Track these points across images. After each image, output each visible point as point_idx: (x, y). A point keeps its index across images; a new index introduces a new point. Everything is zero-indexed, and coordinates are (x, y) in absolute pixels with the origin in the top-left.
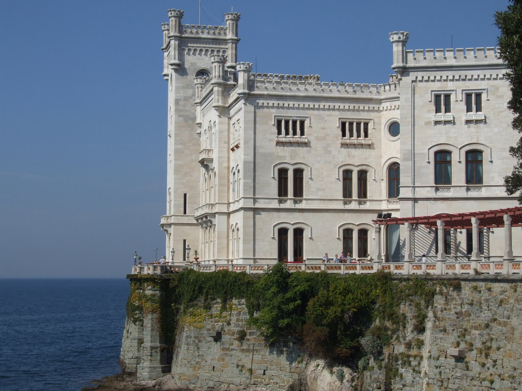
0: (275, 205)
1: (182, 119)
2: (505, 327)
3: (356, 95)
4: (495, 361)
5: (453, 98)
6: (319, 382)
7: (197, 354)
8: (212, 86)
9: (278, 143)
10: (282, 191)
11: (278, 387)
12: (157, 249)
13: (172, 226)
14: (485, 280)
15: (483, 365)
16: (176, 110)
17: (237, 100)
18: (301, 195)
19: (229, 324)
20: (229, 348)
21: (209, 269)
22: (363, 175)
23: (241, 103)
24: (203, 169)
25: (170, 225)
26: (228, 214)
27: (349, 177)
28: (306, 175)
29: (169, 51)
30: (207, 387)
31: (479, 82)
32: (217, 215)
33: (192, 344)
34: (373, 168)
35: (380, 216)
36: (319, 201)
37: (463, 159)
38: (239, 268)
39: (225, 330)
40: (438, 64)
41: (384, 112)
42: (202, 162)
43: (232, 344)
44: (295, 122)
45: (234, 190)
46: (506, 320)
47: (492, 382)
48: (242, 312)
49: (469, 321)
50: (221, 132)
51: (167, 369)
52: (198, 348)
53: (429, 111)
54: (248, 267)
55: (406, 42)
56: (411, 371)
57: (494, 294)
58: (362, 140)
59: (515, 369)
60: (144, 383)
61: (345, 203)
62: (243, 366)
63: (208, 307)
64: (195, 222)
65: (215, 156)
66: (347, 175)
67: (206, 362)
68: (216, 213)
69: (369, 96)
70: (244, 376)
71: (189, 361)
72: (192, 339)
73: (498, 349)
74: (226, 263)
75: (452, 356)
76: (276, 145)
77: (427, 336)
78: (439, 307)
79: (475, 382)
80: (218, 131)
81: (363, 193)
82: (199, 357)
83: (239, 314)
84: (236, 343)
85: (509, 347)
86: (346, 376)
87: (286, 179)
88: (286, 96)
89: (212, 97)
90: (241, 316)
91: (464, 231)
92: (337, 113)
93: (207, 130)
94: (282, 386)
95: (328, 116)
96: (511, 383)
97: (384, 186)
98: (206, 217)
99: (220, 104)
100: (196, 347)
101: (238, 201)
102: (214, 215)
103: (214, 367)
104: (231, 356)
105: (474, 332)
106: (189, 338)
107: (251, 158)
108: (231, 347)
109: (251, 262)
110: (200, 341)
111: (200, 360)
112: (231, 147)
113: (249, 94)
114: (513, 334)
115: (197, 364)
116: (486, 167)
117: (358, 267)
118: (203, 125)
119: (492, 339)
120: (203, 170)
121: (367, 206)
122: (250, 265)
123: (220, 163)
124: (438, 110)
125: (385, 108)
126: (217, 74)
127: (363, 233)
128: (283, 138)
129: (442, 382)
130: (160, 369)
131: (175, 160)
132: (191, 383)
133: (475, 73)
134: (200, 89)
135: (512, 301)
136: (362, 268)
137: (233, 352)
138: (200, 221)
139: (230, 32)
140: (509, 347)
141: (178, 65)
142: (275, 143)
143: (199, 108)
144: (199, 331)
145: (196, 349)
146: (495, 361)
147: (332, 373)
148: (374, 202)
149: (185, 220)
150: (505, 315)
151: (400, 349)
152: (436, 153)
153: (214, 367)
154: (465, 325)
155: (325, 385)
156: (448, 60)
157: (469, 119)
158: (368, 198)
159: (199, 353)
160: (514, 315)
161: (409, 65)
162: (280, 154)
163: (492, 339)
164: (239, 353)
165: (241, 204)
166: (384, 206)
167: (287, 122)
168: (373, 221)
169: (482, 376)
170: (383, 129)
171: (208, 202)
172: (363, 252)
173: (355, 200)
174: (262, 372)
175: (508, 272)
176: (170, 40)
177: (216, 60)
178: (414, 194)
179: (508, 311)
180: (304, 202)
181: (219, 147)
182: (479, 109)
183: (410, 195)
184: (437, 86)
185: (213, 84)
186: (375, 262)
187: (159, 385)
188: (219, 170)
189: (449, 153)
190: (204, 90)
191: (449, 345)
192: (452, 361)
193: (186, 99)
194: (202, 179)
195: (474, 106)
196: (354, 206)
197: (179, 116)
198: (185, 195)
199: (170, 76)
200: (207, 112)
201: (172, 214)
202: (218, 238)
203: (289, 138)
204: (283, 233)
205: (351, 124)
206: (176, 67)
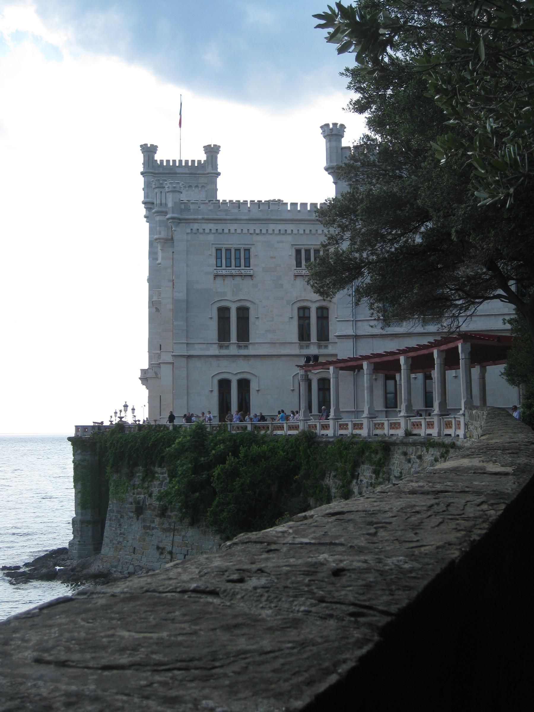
0: (214, 350)
7: (119, 532)
9: (216, 276)
14: (414, 444)
19: (150, 495)
20: (150, 526)
30: (127, 571)
32: (162, 365)
33: (115, 519)
39: (147, 504)
43: (153, 522)
48: (164, 483)
51: (98, 546)
52: (120, 525)
57: (425, 465)
61: (301, 347)
62: (163, 549)
63: (131, 475)
67: (127, 541)
71: (110, 540)
72: (115, 514)
76: (215, 279)
78: (365, 481)
82: (121, 536)
83: (161, 485)
84: (157, 520)
88: (225, 220)
90: (163, 487)
92: (290, 238)
95: (278, 242)
100: (118, 524)
104: (152, 535)
106: (111, 512)
107: (182, 296)
108: (153, 525)
111: (121, 540)
113: (180, 219)
115: (118, 544)
126: (158, 201)
130: (91, 547)
132: (112, 567)
137: (154, 531)
139: (209, 166)
144: (122, 505)
145: (118, 526)
158: (330, 342)
159: (120, 530)
162: (219, 290)
164: (160, 533)
173: (314, 344)
177: (156, 186)
178: (356, 329)
180: (250, 347)
183: (351, 332)
203: (230, 270)
206: (149, 206)
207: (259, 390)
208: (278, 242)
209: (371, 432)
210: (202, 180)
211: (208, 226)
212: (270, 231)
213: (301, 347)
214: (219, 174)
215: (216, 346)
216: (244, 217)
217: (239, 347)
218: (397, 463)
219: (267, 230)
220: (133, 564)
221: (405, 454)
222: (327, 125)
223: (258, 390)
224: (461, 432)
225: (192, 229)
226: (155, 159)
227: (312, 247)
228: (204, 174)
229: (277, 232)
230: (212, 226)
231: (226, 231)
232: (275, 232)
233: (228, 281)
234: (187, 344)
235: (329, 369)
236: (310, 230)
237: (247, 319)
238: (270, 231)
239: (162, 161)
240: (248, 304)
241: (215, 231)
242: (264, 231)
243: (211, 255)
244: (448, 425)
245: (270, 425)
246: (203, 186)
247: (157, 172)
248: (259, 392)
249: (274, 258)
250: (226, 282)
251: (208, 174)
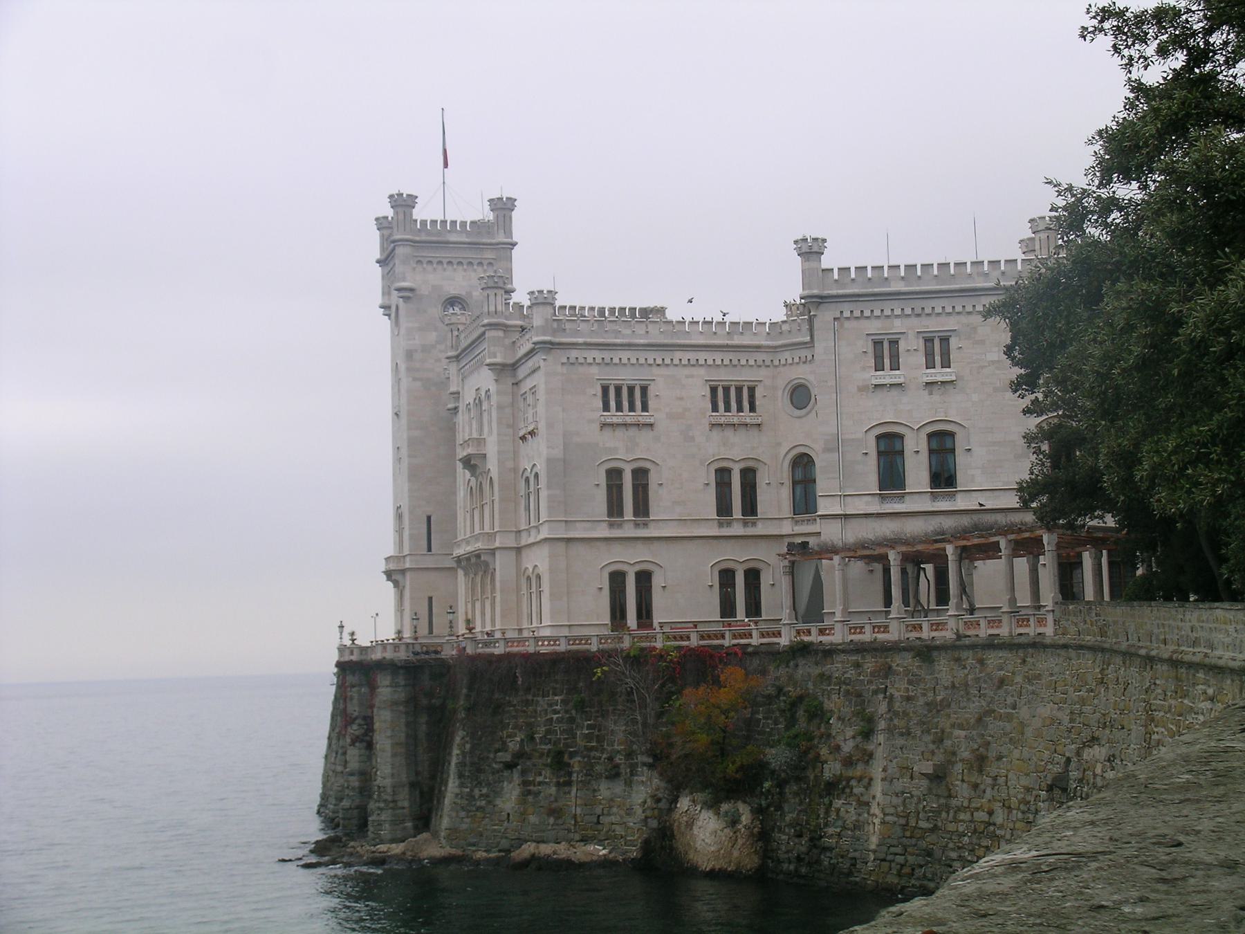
0: (603, 532)
1: (419, 384)
2: (1009, 722)
3: (733, 340)
4: (995, 778)
5: (902, 346)
6: (695, 830)
8: (483, 329)
9: (604, 426)
10: (615, 507)
11: (623, 843)
12: (377, 614)
13: (408, 575)
15: (975, 786)
16: (409, 370)
17: (530, 354)
18: (647, 514)
21: (495, 647)
22: (749, 475)
23: (537, 360)
24: (464, 472)
25: (403, 572)
26: (519, 550)
27: (726, 480)
28: (653, 479)
29: (391, 265)
31: (943, 319)
34: (765, 464)
35: (790, 545)
36: (676, 523)
37: (923, 446)
38: (546, 643)
40: (876, 290)
41: (781, 369)
42: (468, 463)
44: (631, 390)
45: (528, 509)
46: (1011, 711)
47: (991, 813)
49: (949, 716)
50: (500, 408)
53: (864, 369)
54: (563, 641)
55: (823, 254)
56: (854, 803)
58: (747, 416)
59: (1028, 790)
60: (383, 847)
64: (454, 565)
65: (491, 449)
66: (723, 475)
68: (497, 548)
69: (755, 342)
70: (562, 827)
73: (999, 758)
74: (515, 635)
75: (922, 774)
77: (880, 744)
79: (962, 816)
80: (495, 406)
81: (750, 507)
85: (1016, 754)
86: (743, 818)
87: (620, 487)
89: (485, 345)
91: (929, 568)
92: (702, 371)
93: (472, 403)
94: (630, 840)
95: (687, 377)
96: (1023, 812)
97: (786, 493)
98: (478, 556)
99: (498, 360)
101: (536, 527)
102: (493, 552)
103: (509, 814)
105: (957, 732)
108: (540, 779)
109: (565, 632)
110: (479, 771)
112: (521, 433)
114: (1023, 734)
116: (961, 458)
117: (755, 633)
118: (463, 397)
119: (989, 743)
120: (463, 475)
121: (760, 529)
122: (566, 637)
123: (501, 463)
124: (879, 367)
125: (783, 362)
126: (492, 309)
127: (753, 576)
128: (614, 417)
129: (907, 816)
131: (409, 456)
133: (938, 305)
134: (456, 333)
135: (1019, 679)
136: (762, 635)
138: (463, 564)
140: (1016, 754)
141: (411, 290)
142: (599, 429)
143: (453, 368)
146: (995, 778)
147: (717, 814)
148: (769, 522)
149: (429, 562)
150: (1008, 702)
151: (832, 769)
152: (878, 438)
153: (509, 814)
154: (944, 723)
155: (708, 834)
156: (892, 283)
157: (930, 379)
158: (759, 517)
160: (1023, 702)
161: (826, 292)
163: (989, 743)
165: (544, 534)
166: (787, 528)
167: (618, 390)
168: (779, 555)
169: (973, 805)
170: (780, 399)
171: (477, 531)
172: (754, 608)
174: (595, 820)
175: (1011, 632)
176: (395, 246)
178: (845, 506)
179: (1012, 696)
180: (652, 525)
181: (498, 435)
182: (946, 364)
184: (874, 327)
185: (483, 326)
186: (784, 624)
187: (412, 851)
188: (500, 473)
189: (901, 437)
190: (462, 336)
191: (917, 758)
192: (925, 783)
193: (426, 349)
194: (462, 493)
195: (938, 358)
196: (737, 530)
197: (415, 379)
198: (429, 518)
199: (394, 309)
200: (472, 372)
201: (406, 552)
202: (502, 591)
204: (617, 579)
205: (726, 390)
207: (665, 587)
208: (687, 377)
209: (902, 635)
210: (489, 255)
211: (591, 355)
212: (676, 362)
213: (721, 525)
214: (514, 244)
215: (605, 525)
216: (642, 341)
217: (637, 525)
218: (946, 671)
219: (672, 360)
220: (506, 838)
221: (958, 660)
222: (805, 240)
223: (664, 587)
224: (1049, 630)
225: (568, 358)
226: (414, 218)
227: (733, 383)
228: (491, 244)
229: (685, 362)
230: (598, 355)
231: (616, 360)
232: (683, 362)
233: (620, 433)
234: (566, 521)
235: (832, 559)
236: (731, 360)
237: (645, 487)
238: (676, 362)
239: (424, 223)
240: (647, 465)
241: (600, 361)
242: (668, 361)
243: (595, 395)
244: (1024, 621)
245: (727, 633)
246: (490, 264)
247: (417, 238)
248: (666, 589)
249: (681, 399)
250: (616, 433)
251: (498, 244)
